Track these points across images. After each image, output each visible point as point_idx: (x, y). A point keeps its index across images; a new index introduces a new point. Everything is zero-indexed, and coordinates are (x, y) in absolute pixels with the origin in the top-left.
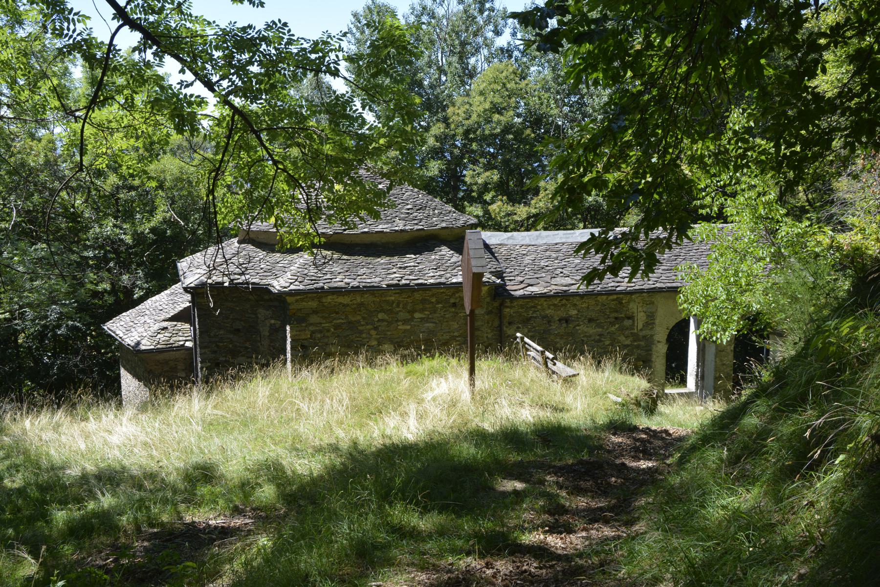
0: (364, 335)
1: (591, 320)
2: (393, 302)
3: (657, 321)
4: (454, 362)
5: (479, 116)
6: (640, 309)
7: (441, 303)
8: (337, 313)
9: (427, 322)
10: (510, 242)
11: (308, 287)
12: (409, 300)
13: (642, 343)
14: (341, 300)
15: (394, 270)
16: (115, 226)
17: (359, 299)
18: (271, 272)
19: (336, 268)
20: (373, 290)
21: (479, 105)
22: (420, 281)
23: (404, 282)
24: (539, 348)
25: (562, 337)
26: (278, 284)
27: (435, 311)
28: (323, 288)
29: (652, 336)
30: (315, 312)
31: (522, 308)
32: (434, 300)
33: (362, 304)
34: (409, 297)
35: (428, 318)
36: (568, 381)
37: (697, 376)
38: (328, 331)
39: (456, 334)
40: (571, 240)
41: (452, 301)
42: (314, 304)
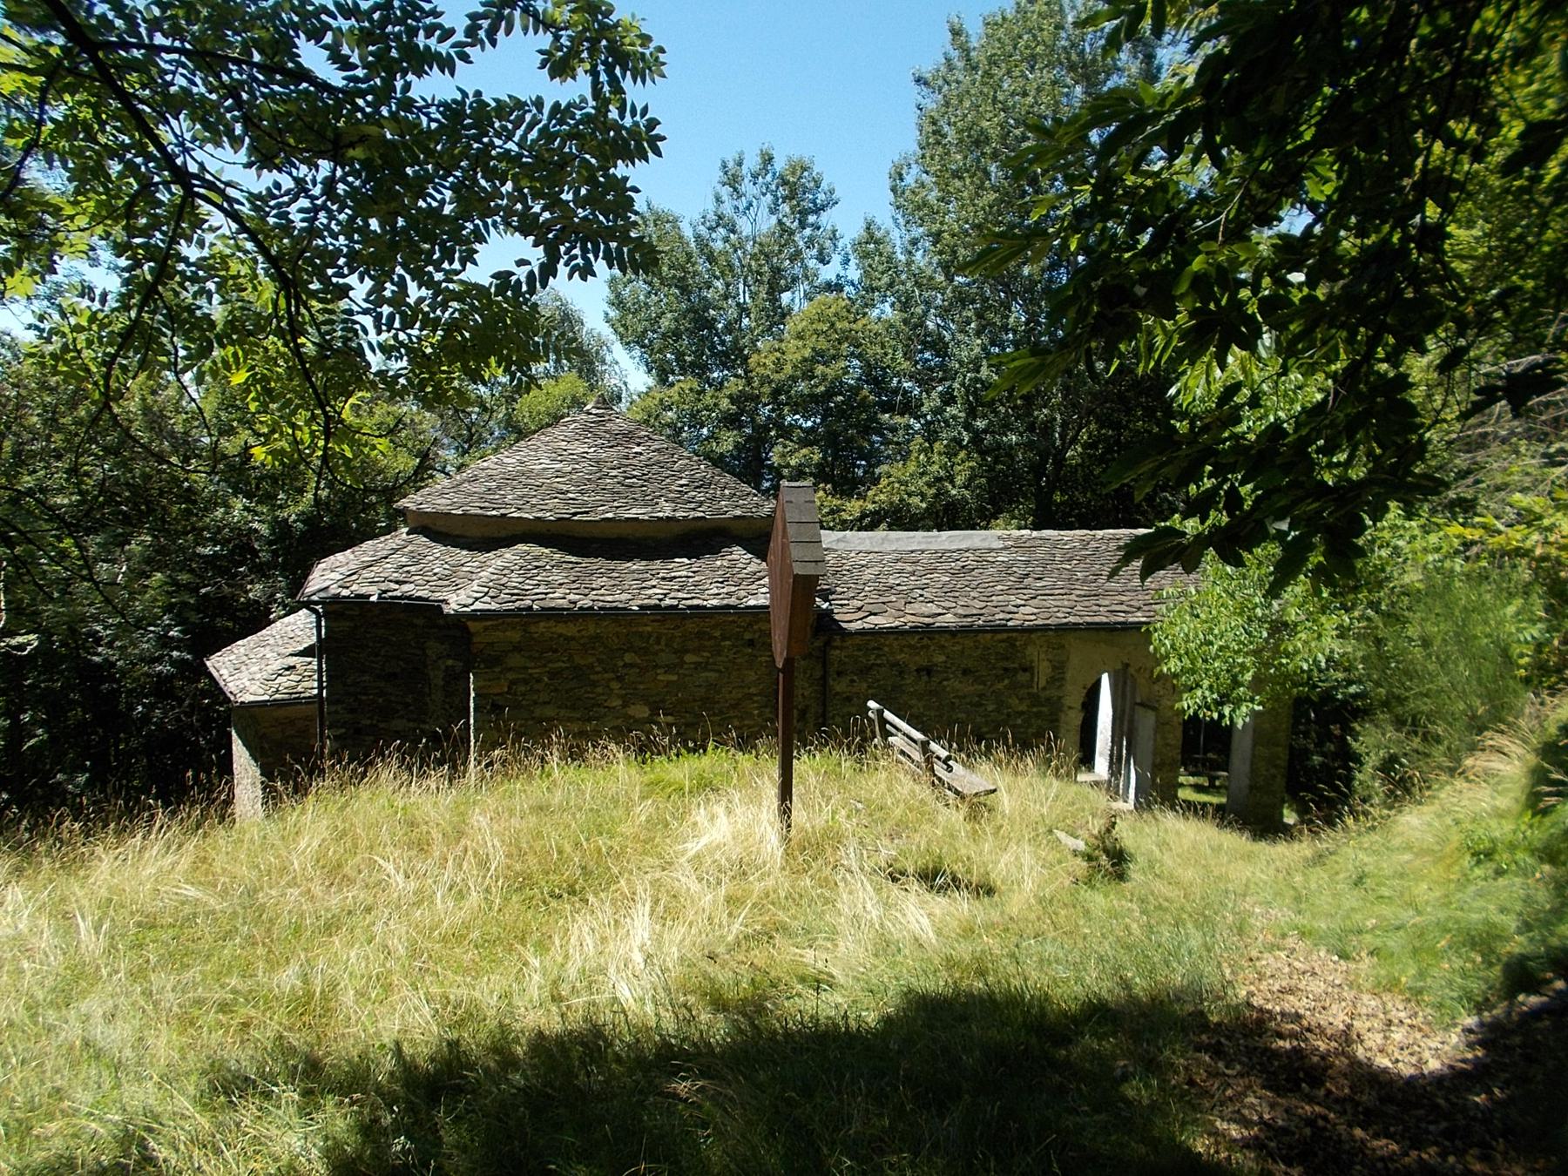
0: (600, 690)
1: (965, 672)
2: (650, 635)
3: (1068, 676)
4: (745, 760)
5: (795, 366)
6: (1042, 656)
7: (729, 639)
8: (555, 651)
9: (706, 669)
10: (841, 546)
11: (505, 606)
12: (677, 633)
13: (1044, 709)
14: (560, 629)
15: (654, 583)
16: (246, 509)
17: (592, 629)
18: (451, 579)
19: (557, 576)
20: (616, 614)
21: (796, 352)
22: (695, 602)
23: (668, 602)
24: (918, 735)
26: (456, 601)
28: (531, 608)
29: (1060, 698)
30: (517, 648)
32: (717, 634)
33: (597, 637)
36: (978, 806)
37: (1111, 756)
38: (539, 681)
40: (934, 547)
41: (747, 636)
42: (515, 636)
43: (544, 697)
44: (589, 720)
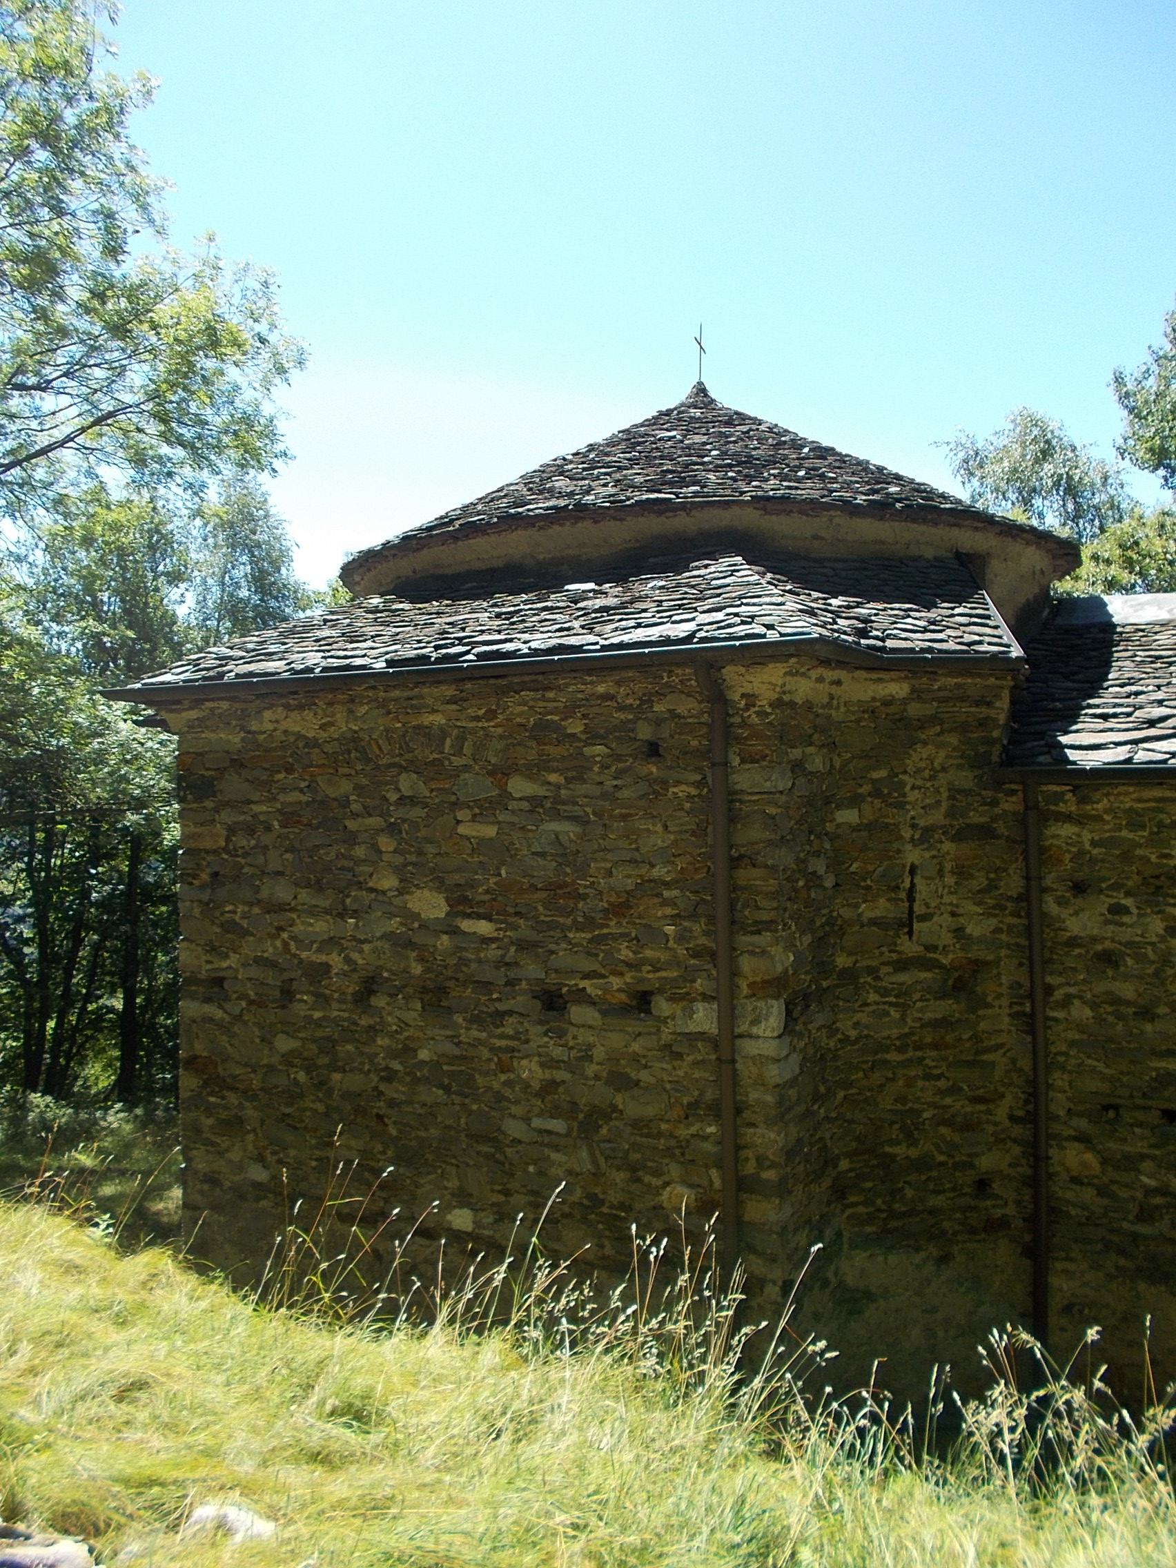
0: (360, 852)
2: (444, 733)
8: (289, 770)
9: (557, 815)
27: (578, 771)
31: (1135, 826)
33: (354, 740)
34: (490, 715)
35: (557, 800)
39: (659, 872)
41: (645, 732)
43: (274, 863)
44: (342, 916)
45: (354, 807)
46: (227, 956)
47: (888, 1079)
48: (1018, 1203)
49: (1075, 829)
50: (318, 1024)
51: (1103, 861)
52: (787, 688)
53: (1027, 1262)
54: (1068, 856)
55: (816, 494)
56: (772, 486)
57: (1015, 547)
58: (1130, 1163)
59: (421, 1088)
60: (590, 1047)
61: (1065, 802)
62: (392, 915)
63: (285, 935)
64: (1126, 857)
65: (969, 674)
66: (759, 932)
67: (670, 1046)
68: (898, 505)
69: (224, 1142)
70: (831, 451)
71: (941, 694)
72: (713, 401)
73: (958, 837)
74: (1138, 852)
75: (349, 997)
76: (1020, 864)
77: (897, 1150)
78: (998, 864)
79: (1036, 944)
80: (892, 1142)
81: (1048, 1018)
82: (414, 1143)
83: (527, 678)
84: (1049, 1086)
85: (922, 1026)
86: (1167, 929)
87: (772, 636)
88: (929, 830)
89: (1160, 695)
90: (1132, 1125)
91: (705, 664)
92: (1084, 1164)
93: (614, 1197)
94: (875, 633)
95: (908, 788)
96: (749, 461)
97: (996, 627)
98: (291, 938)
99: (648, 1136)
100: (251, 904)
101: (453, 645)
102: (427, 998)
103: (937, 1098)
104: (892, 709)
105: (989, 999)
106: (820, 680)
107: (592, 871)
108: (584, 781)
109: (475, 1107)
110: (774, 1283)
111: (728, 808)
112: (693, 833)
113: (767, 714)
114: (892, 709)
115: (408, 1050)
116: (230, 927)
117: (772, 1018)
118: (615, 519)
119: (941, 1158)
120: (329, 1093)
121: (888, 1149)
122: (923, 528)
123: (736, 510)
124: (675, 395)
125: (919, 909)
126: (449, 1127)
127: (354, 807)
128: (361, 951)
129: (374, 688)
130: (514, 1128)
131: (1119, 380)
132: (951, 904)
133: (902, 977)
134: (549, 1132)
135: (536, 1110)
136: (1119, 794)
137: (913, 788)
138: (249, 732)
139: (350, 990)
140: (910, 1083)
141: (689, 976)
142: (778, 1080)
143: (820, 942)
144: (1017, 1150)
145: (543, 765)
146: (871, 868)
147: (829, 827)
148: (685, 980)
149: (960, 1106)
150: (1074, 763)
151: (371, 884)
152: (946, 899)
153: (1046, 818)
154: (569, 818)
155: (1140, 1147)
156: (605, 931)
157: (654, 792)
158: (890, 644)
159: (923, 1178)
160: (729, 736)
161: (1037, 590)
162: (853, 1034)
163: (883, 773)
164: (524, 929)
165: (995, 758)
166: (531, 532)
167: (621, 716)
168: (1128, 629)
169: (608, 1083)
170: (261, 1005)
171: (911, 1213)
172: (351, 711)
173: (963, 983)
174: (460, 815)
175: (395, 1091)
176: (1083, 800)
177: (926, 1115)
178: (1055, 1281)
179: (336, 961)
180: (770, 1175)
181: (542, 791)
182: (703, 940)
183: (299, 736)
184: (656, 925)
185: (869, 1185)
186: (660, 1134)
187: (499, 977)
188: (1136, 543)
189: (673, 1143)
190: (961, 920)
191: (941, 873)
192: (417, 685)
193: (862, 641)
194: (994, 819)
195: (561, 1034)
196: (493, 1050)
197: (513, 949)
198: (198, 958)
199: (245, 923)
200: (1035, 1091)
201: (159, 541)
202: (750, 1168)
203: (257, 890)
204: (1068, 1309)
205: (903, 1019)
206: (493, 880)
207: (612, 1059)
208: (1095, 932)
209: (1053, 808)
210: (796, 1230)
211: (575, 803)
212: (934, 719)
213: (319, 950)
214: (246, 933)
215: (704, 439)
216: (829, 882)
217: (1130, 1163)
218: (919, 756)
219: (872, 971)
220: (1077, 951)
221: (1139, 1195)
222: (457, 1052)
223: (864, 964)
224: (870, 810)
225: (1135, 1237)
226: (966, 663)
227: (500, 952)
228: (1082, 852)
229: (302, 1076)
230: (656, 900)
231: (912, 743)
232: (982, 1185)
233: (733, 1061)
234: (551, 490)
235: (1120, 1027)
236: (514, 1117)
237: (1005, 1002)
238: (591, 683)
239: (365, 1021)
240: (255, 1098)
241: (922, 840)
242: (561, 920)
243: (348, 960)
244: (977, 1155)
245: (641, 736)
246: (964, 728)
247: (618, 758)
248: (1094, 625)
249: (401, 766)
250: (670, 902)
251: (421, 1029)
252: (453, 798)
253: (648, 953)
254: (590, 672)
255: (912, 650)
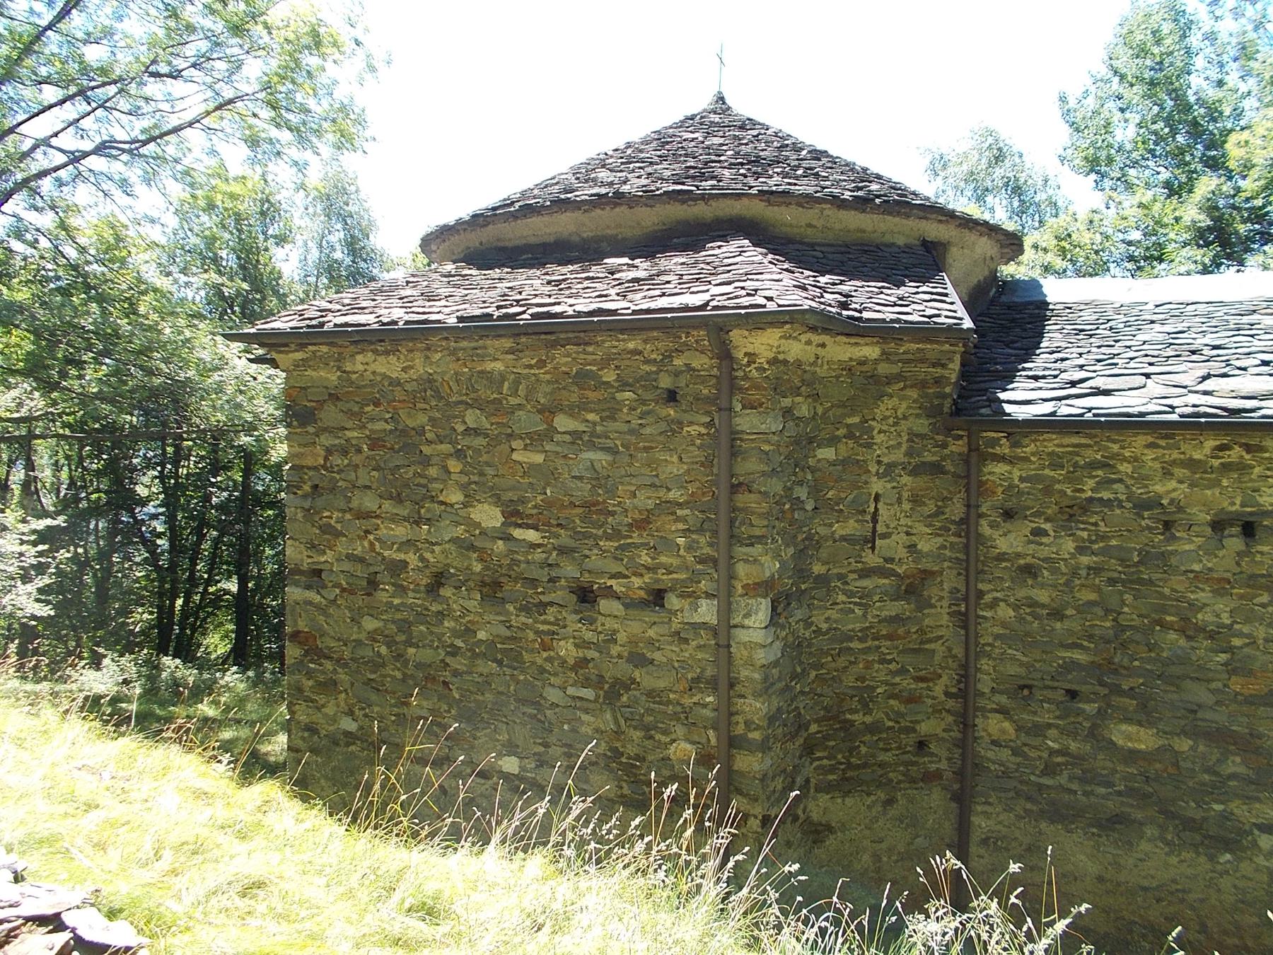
0: (433, 472)
2: (503, 378)
8: (377, 404)
9: (592, 446)
25: (1222, 587)
27: (611, 413)
31: (1055, 466)
34: (541, 364)
35: (593, 434)
39: (674, 495)
41: (665, 382)
45: (429, 436)
46: (325, 553)
47: (851, 663)
48: (949, 759)
49: (1008, 468)
50: (397, 609)
51: (1028, 493)
52: (781, 349)
53: (954, 805)
54: (1000, 489)
55: (811, 190)
56: (774, 182)
57: (970, 237)
58: (1038, 730)
59: (479, 662)
60: (615, 632)
61: (1001, 446)
62: (458, 524)
63: (371, 537)
64: (1048, 491)
65: (928, 340)
66: (752, 545)
67: (679, 633)
68: (877, 201)
69: (321, 699)
70: (825, 153)
71: (905, 357)
72: (729, 108)
73: (914, 472)
74: (1057, 487)
75: (422, 588)
76: (963, 495)
77: (855, 717)
78: (945, 493)
79: (971, 557)
80: (853, 711)
81: (978, 617)
82: (473, 705)
83: (571, 335)
84: (978, 670)
85: (879, 622)
86: (1077, 548)
87: (771, 306)
88: (891, 466)
89: (1081, 361)
90: (1042, 701)
91: (716, 328)
92: (1003, 731)
93: (631, 750)
94: (853, 306)
95: (875, 432)
96: (757, 161)
97: (952, 303)
98: (376, 539)
99: (660, 703)
100: (344, 511)
101: (512, 305)
102: (485, 590)
103: (889, 678)
104: (864, 368)
105: (933, 601)
106: (809, 343)
107: (619, 493)
108: (615, 420)
109: (522, 678)
110: (756, 817)
111: (733, 445)
112: (702, 465)
113: (765, 370)
114: (864, 368)
115: (469, 632)
116: (327, 529)
117: (761, 611)
118: (647, 205)
119: (891, 724)
120: (406, 662)
121: (848, 716)
122: (897, 219)
123: (745, 201)
124: (699, 102)
125: (880, 529)
126: (502, 693)
127: (429, 436)
128: (433, 552)
129: (447, 339)
130: (553, 695)
131: (1063, 99)
132: (906, 526)
133: (867, 583)
134: (581, 699)
135: (571, 681)
136: (1045, 440)
137: (880, 432)
138: (344, 372)
139: (424, 582)
140: (868, 665)
141: (695, 578)
142: (764, 662)
143: (801, 553)
144: (950, 719)
145: (584, 406)
146: (843, 495)
147: (811, 462)
148: (692, 581)
149: (907, 684)
150: (1009, 415)
151: (441, 498)
152: (902, 522)
153: (985, 458)
154: (602, 449)
155: (1047, 718)
156: (629, 541)
157: (672, 430)
158: (866, 315)
159: (875, 738)
160: (733, 388)
161: (987, 273)
162: (824, 626)
163: (856, 420)
164: (565, 538)
165: (946, 410)
166: (578, 214)
167: (647, 368)
168: (1058, 307)
169: (628, 661)
170: (352, 592)
171: (865, 765)
172: (427, 357)
173: (913, 588)
174: (515, 444)
175: (458, 663)
176: (1015, 445)
177: (879, 690)
178: (975, 820)
179: (412, 559)
180: (756, 735)
181: (582, 428)
182: (707, 550)
183: (384, 376)
184: (671, 537)
185: (832, 743)
186: (669, 702)
187: (543, 575)
188: (1069, 235)
189: (679, 709)
190: (914, 538)
191: (899, 501)
192: (481, 337)
193: (845, 313)
194: (943, 459)
195: (592, 621)
196: (537, 632)
197: (555, 554)
198: (301, 553)
199: (339, 527)
200: (966, 674)
201: (268, 210)
202: (740, 730)
203: (349, 500)
204: (985, 841)
205: (864, 616)
206: (540, 497)
207: (633, 642)
208: (1020, 549)
209: (990, 450)
210: (773, 778)
211: (607, 437)
212: (899, 377)
213: (398, 550)
214: (339, 534)
215: (722, 141)
216: (809, 507)
217: (1038, 730)
218: (885, 407)
219: (841, 577)
220: (1004, 564)
221: (1045, 755)
222: (508, 633)
223: (835, 571)
224: (844, 449)
225: (1040, 787)
226: (926, 332)
227: (544, 555)
228: (1011, 487)
229: (384, 650)
230: (671, 517)
231: (881, 397)
232: (921, 745)
233: (729, 646)
234: (594, 180)
235: (1036, 625)
236: (553, 686)
237: (945, 603)
238: (623, 340)
239: (435, 608)
240: (346, 665)
241: (885, 475)
242: (594, 531)
243: (422, 559)
244: (918, 722)
245: (662, 385)
246: (923, 385)
247: (644, 402)
248: (1031, 303)
249: (467, 403)
250: (683, 519)
251: (481, 615)
252: (509, 431)
253: (663, 559)
254: (622, 331)
255: (884, 321)
